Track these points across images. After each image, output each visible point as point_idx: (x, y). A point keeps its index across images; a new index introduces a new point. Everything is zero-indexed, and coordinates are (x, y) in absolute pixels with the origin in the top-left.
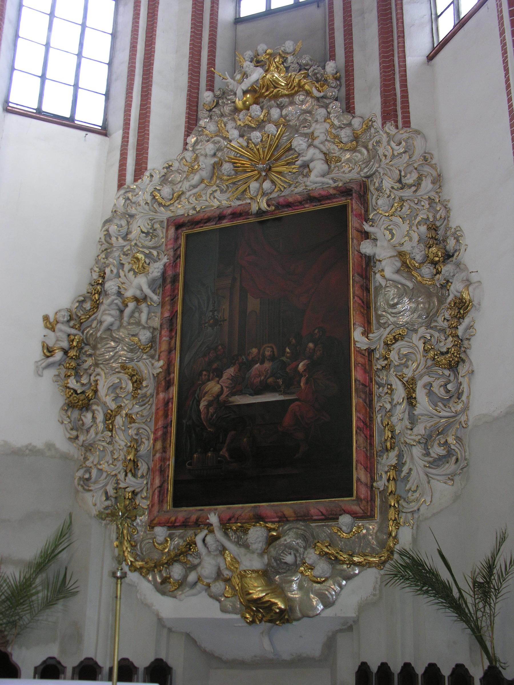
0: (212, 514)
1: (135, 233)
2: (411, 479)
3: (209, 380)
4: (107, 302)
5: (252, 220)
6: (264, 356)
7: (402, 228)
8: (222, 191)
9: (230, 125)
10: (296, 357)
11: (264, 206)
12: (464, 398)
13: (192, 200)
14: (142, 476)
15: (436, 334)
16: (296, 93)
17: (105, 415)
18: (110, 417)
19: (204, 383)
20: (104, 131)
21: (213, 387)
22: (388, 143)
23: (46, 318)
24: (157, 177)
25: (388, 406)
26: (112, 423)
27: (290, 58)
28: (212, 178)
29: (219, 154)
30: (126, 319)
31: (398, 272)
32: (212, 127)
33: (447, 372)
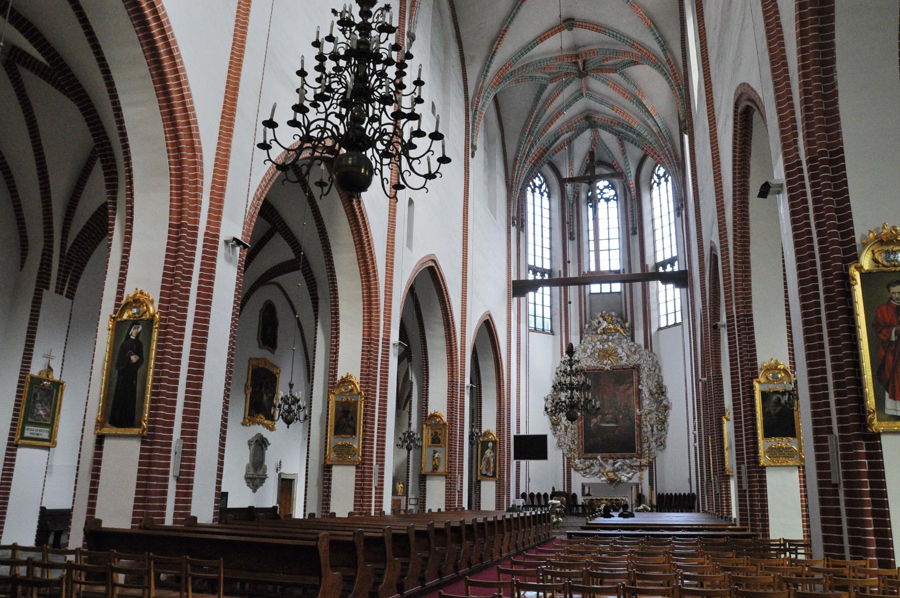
18: (566, 428)
20: (552, 332)
21: (594, 420)
32: (589, 338)
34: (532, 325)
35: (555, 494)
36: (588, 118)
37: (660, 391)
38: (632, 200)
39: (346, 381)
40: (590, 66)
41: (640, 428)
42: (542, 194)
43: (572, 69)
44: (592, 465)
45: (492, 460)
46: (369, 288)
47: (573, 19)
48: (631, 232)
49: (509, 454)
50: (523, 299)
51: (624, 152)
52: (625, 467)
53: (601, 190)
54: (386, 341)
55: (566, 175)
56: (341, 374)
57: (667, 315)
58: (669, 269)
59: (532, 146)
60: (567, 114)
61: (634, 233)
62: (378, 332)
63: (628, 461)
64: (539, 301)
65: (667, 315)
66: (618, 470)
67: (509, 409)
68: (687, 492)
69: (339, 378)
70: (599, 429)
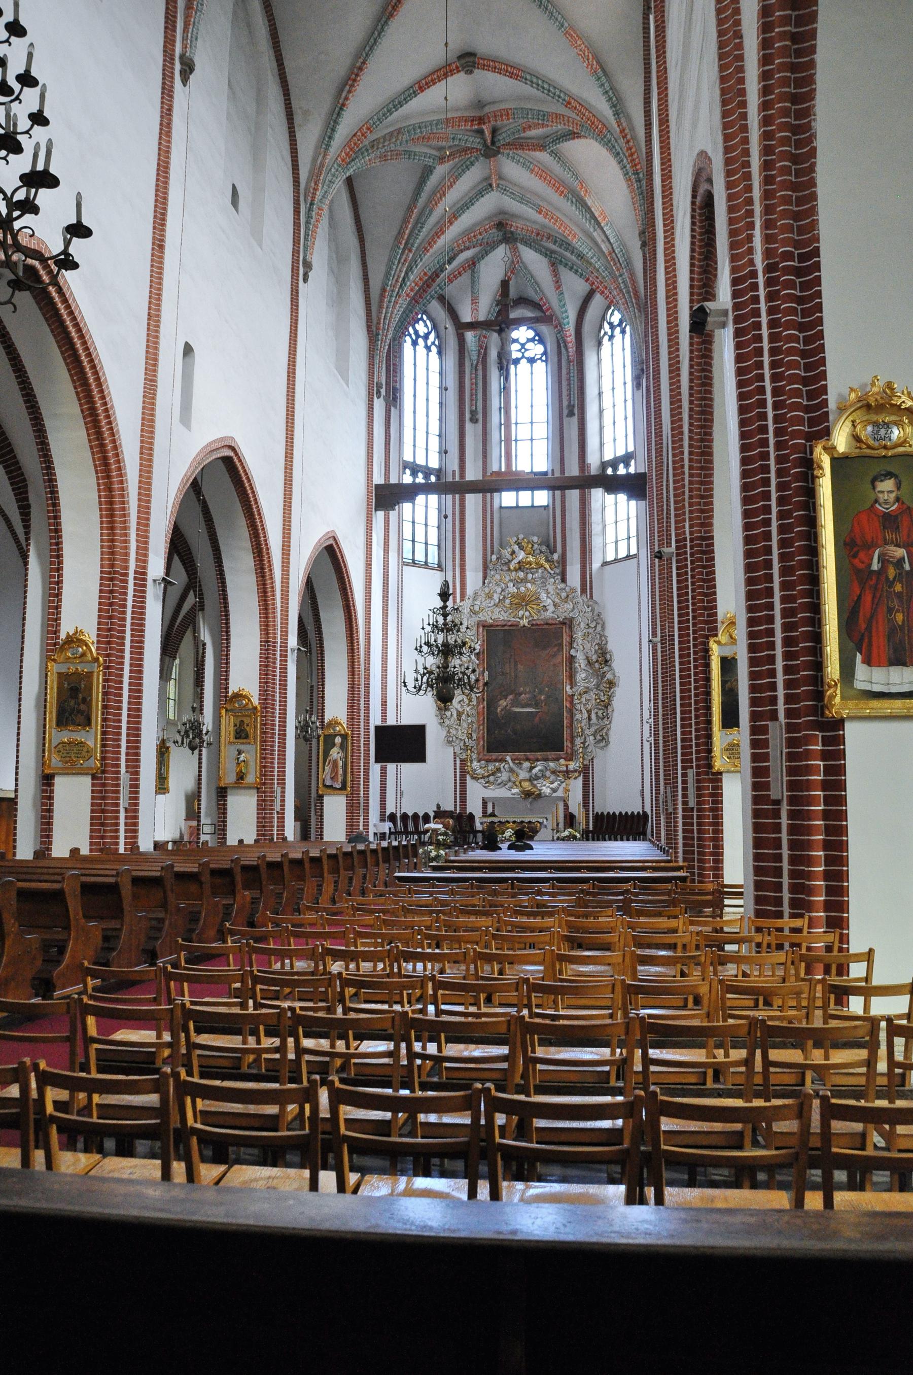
10: (541, 693)
18: (459, 714)
21: (503, 703)
27: (536, 546)
32: (497, 577)
34: (408, 555)
35: (440, 814)
36: (500, 225)
37: (604, 658)
38: (569, 361)
39: (74, 640)
40: (502, 138)
42: (428, 348)
43: (474, 142)
44: (498, 770)
45: (340, 764)
46: (110, 489)
47: (472, 54)
48: (565, 412)
49: (367, 755)
50: (393, 514)
51: (558, 284)
52: (548, 773)
53: (523, 345)
54: (141, 575)
55: (466, 317)
56: (66, 628)
57: (616, 542)
58: (622, 471)
59: (410, 269)
60: (466, 220)
61: (571, 414)
62: (127, 561)
63: (552, 764)
64: (420, 518)
65: (616, 542)
66: (537, 778)
68: (636, 809)
69: (63, 635)
70: (512, 717)
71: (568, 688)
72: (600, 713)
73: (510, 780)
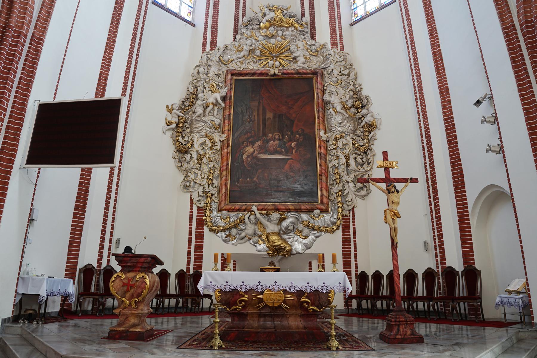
0: (254, 206)
1: (211, 74)
2: (348, 196)
3: (247, 146)
4: (199, 102)
5: (268, 77)
6: (275, 138)
7: (341, 92)
8: (254, 62)
9: (258, 34)
10: (291, 140)
11: (276, 72)
12: (371, 164)
13: (239, 64)
14: (216, 187)
15: (357, 138)
16: (290, 27)
17: (198, 157)
18: (200, 158)
19: (245, 147)
21: (250, 149)
22: (334, 55)
23: (167, 107)
24: (221, 51)
25: (337, 165)
26: (201, 161)
27: (285, 12)
28: (248, 56)
29: (253, 46)
30: (207, 113)
31: (342, 109)
32: (248, 33)
33: (362, 154)
37: (359, 104)
41: (324, 157)
44: (242, 221)
52: (300, 227)
63: (305, 217)
66: (287, 231)
67: (38, 43)
71: (322, 133)
72: (359, 159)
73: (255, 234)
